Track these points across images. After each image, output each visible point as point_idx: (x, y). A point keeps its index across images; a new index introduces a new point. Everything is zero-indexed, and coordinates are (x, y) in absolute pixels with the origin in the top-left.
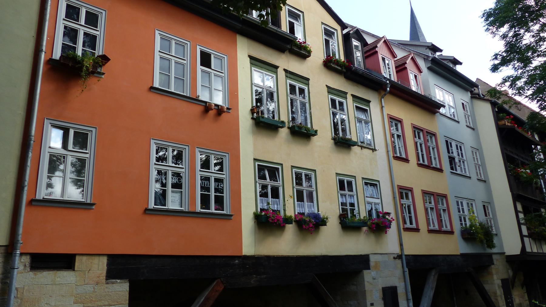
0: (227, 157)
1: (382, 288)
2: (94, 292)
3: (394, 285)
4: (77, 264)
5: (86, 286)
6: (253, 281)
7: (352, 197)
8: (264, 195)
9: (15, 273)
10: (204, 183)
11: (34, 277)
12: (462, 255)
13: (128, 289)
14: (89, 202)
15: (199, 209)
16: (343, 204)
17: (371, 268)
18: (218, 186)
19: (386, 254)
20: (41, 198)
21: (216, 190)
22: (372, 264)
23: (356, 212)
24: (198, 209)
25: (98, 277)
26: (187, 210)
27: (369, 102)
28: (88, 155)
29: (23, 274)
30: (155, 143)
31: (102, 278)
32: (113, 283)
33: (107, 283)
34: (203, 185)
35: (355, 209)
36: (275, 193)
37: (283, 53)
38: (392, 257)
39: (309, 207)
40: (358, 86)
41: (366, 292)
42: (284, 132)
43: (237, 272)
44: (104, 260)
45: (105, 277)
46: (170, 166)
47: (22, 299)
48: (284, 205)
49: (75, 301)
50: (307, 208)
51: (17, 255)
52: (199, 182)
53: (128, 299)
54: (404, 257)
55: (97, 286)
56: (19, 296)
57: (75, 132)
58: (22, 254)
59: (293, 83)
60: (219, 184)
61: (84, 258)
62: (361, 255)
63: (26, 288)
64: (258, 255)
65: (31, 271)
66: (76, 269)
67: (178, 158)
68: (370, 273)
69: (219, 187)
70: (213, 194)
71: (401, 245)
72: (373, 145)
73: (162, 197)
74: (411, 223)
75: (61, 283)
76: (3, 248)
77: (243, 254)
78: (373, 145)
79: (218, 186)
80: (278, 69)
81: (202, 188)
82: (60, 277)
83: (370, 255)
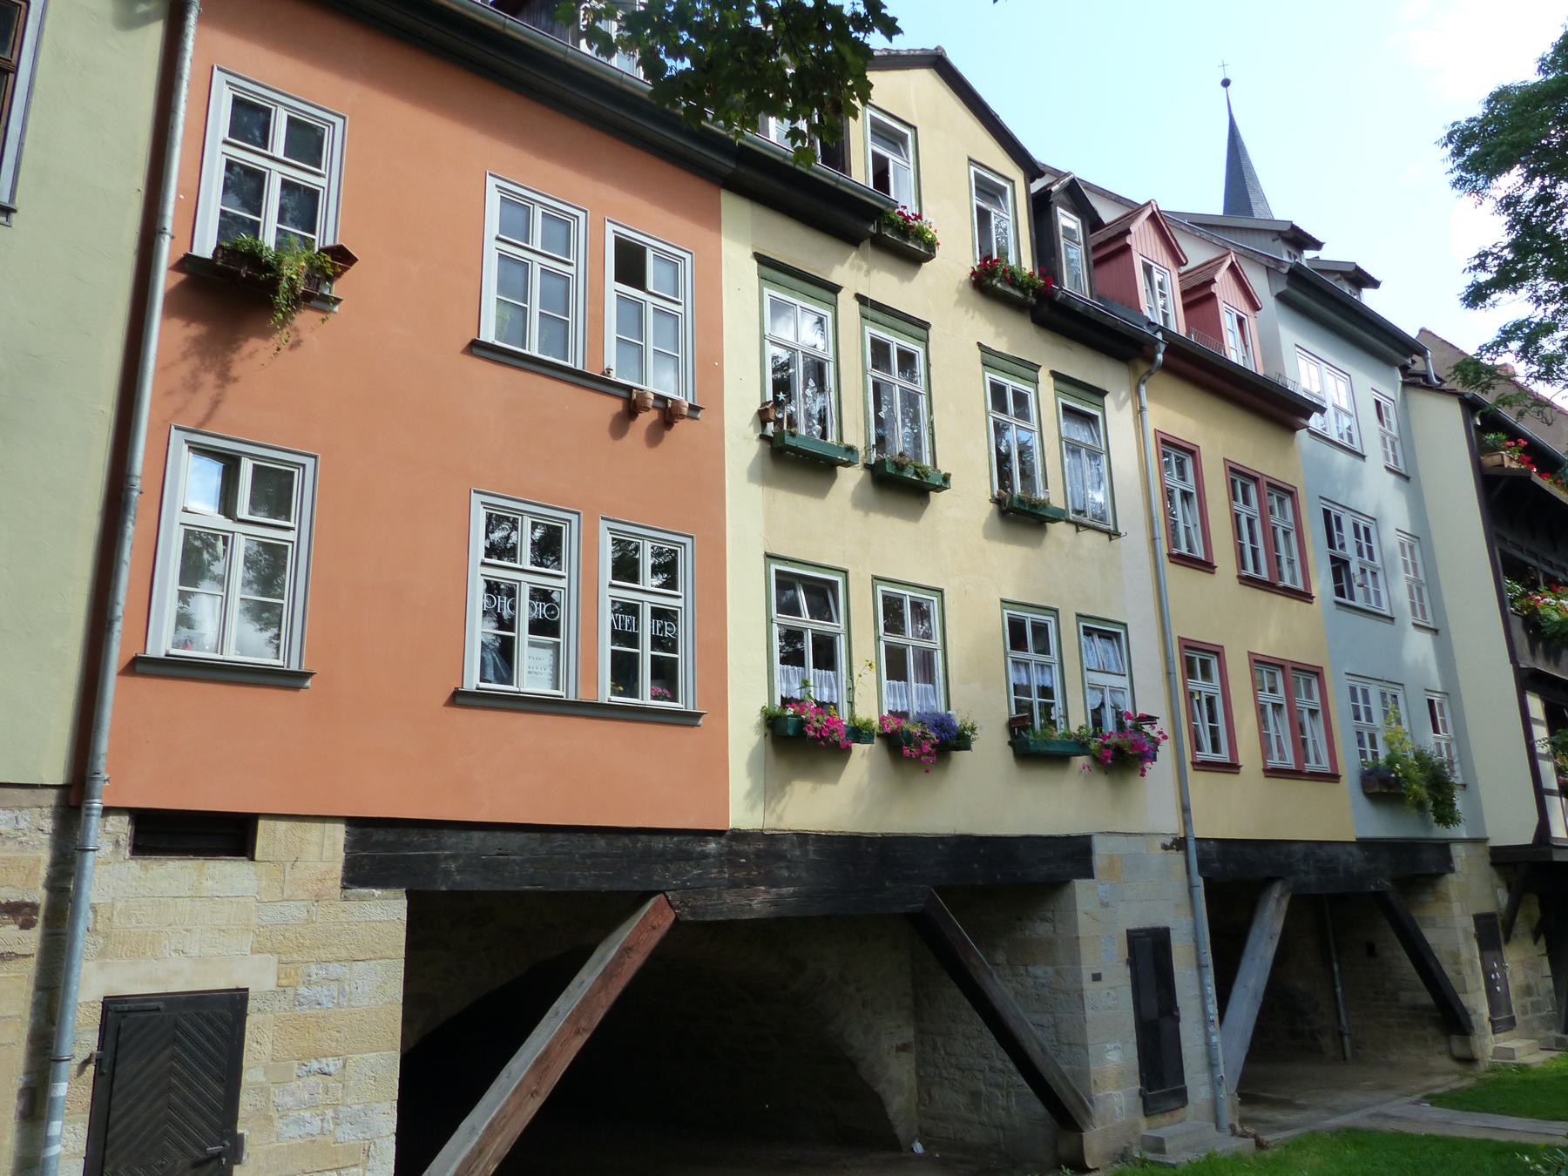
1: (1127, 930)
2: (309, 921)
4: (260, 842)
5: (285, 903)
6: (758, 902)
7: (1046, 670)
8: (793, 657)
10: (623, 622)
11: (142, 876)
12: (1363, 843)
13: (404, 918)
14: (294, 667)
15: (605, 693)
16: (1018, 689)
19: (1141, 834)
20: (162, 655)
21: (657, 642)
22: (1099, 861)
23: (1056, 713)
25: (320, 881)
26: (572, 698)
27: (1101, 393)
28: (289, 534)
29: (110, 867)
30: (482, 503)
31: (330, 883)
32: (361, 898)
33: (346, 899)
34: (618, 627)
35: (1053, 704)
36: (826, 654)
38: (1158, 842)
39: (923, 696)
40: (1069, 348)
41: (1081, 940)
42: (850, 478)
43: (713, 876)
44: (339, 832)
45: (339, 882)
46: (524, 574)
47: (107, 936)
48: (851, 689)
49: (256, 945)
50: (915, 698)
51: (95, 812)
52: (606, 618)
53: (404, 944)
54: (1192, 846)
55: (316, 904)
56: (99, 927)
58: (107, 811)
59: (883, 335)
60: (664, 625)
61: (282, 826)
62: (1068, 838)
63: (119, 905)
65: (132, 859)
66: (258, 856)
67: (549, 546)
69: (664, 634)
70: (646, 652)
71: (1185, 809)
72: (1110, 519)
73: (503, 655)
74: (1216, 748)
76: (54, 792)
77: (731, 826)
78: (1110, 519)
80: (839, 295)
81: (617, 636)
82: (213, 878)
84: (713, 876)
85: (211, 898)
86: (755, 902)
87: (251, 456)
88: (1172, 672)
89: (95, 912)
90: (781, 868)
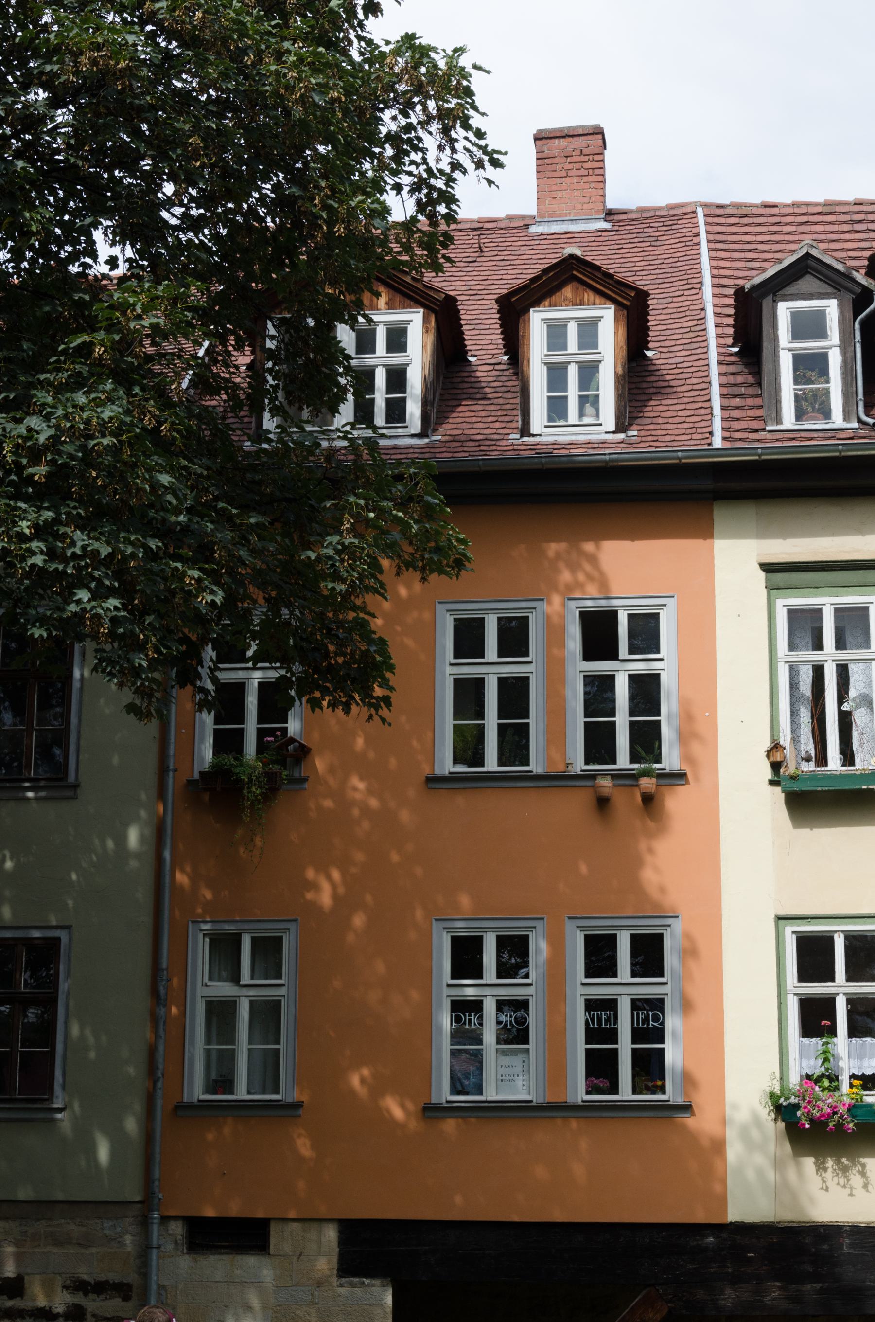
4: (273, 1241)
9: (154, 1257)
10: (600, 1019)
18: (646, 1020)
21: (638, 1035)
26: (541, 1100)
34: (593, 1024)
43: (712, 1270)
45: (335, 1272)
51: (155, 1221)
52: (580, 1016)
56: (169, 1301)
57: (254, 940)
60: (648, 1014)
63: (181, 1286)
64: (788, 1222)
65: (187, 1254)
66: (272, 1251)
69: (648, 1024)
70: (625, 1046)
75: (244, 1280)
79: (646, 1020)
81: (591, 1035)
84: (712, 1270)
85: (242, 1282)
86: (769, 1298)
87: (247, 931)
89: (166, 1291)
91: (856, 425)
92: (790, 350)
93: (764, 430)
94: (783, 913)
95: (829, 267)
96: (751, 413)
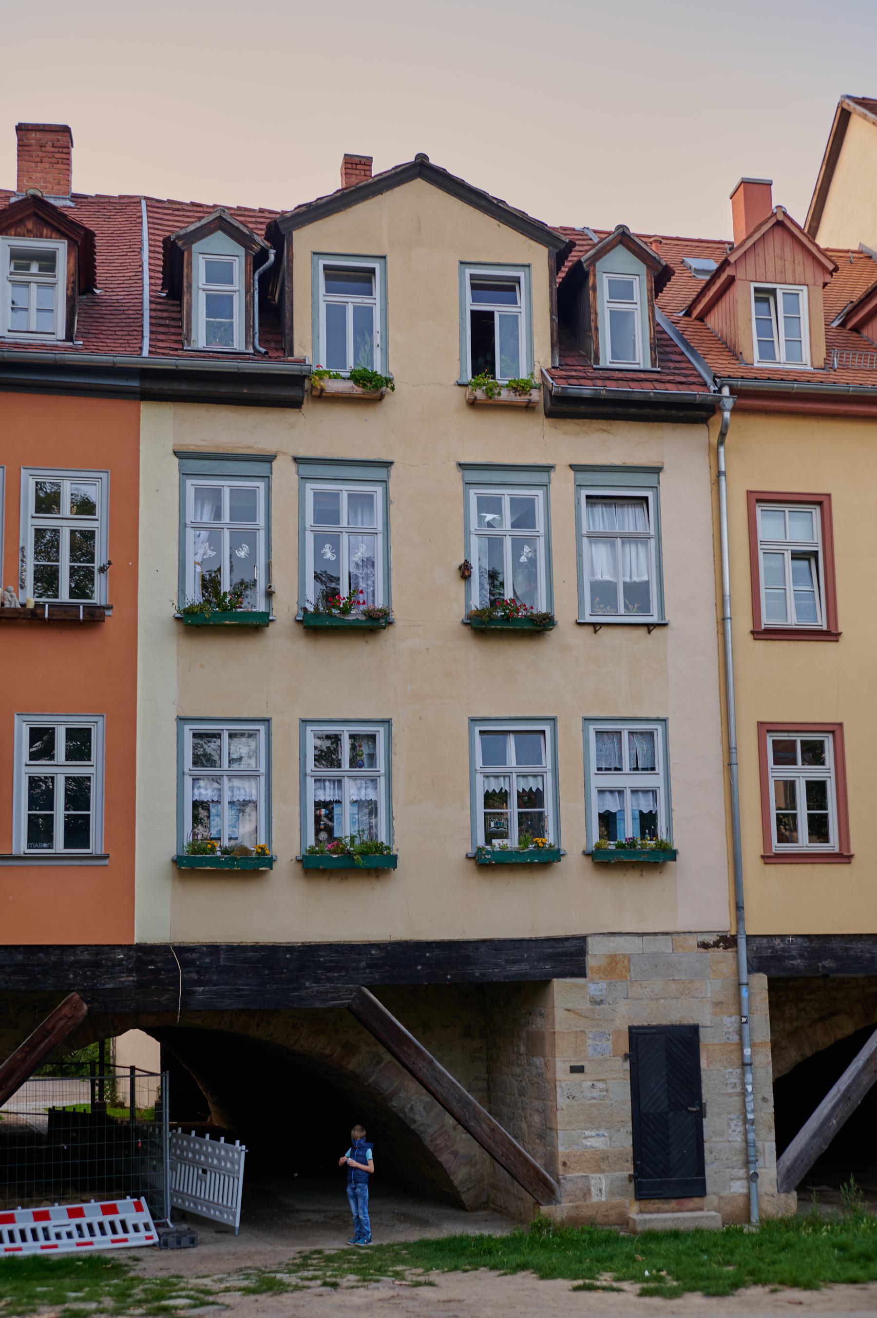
0: (100, 724)
1: (630, 1028)
3: (691, 1022)
7: (507, 779)
17: (588, 972)
19: (667, 934)
22: (591, 962)
24: (20, 851)
37: (298, 410)
38: (693, 941)
41: (556, 1036)
54: (742, 943)
68: (584, 987)
71: (739, 907)
77: (136, 941)
80: (273, 463)
83: (589, 939)
88: (734, 761)
90: (191, 972)
91: (252, 351)
92: (204, 290)
93: (182, 350)
94: (182, 715)
95: (237, 228)
96: (173, 338)
